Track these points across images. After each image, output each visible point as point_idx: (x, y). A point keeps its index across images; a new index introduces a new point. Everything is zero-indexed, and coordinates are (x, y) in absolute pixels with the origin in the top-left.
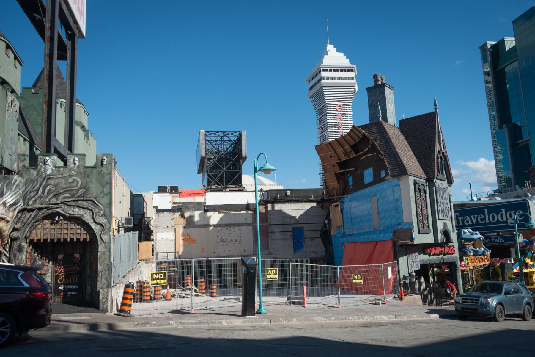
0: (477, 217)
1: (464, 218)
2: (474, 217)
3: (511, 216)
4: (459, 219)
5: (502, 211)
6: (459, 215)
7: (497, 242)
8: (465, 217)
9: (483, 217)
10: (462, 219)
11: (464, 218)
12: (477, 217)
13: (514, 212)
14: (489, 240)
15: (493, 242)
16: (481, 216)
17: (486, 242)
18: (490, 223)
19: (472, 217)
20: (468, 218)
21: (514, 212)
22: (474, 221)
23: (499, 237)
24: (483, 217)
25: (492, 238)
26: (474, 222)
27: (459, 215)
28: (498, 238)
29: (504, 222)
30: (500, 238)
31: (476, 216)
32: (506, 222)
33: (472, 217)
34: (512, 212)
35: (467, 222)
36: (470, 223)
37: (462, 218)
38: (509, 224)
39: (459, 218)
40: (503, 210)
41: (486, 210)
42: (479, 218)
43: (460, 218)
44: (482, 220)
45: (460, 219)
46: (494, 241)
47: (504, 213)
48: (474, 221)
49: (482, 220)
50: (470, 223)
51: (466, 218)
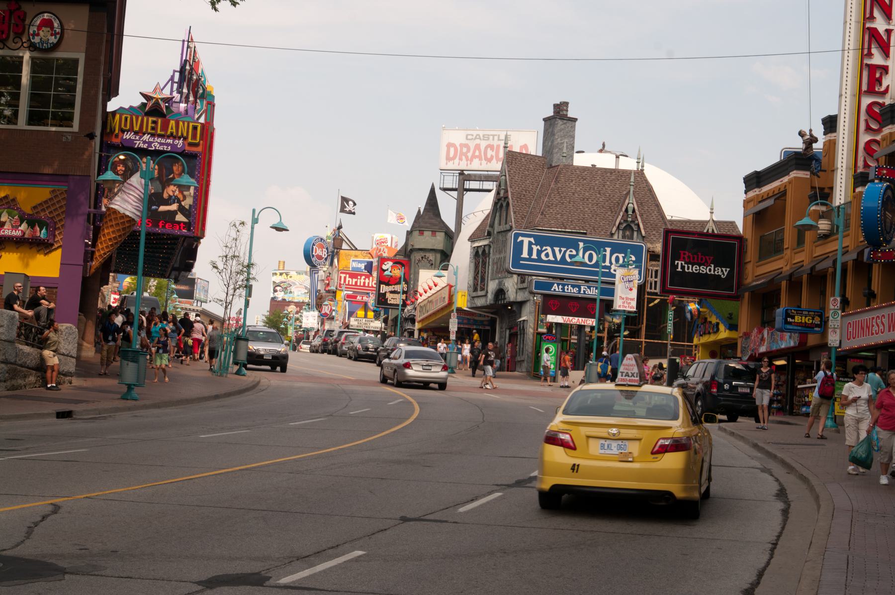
0: (565, 252)
1: (542, 248)
2: (560, 251)
3: (617, 259)
4: (532, 248)
5: (605, 251)
6: (534, 242)
7: (589, 293)
8: (544, 248)
9: (574, 253)
10: (538, 249)
11: (542, 248)
12: (565, 252)
13: (623, 255)
14: (577, 289)
15: (582, 292)
16: (571, 251)
17: (572, 291)
18: (583, 264)
19: (557, 249)
20: (549, 250)
21: (623, 255)
22: (559, 257)
23: (593, 287)
24: (574, 253)
25: (582, 287)
26: (559, 258)
27: (534, 242)
28: (592, 288)
29: (605, 267)
30: (594, 288)
31: (563, 249)
32: (609, 268)
33: (557, 249)
34: (621, 256)
35: (547, 255)
36: (551, 258)
37: (539, 247)
38: (612, 271)
39: (533, 246)
40: (608, 250)
41: (581, 245)
42: (568, 253)
43: (535, 248)
44: (571, 256)
45: (535, 248)
46: (584, 291)
47: (608, 253)
48: (559, 257)
49: (571, 256)
50: (551, 258)
51: (546, 249)
